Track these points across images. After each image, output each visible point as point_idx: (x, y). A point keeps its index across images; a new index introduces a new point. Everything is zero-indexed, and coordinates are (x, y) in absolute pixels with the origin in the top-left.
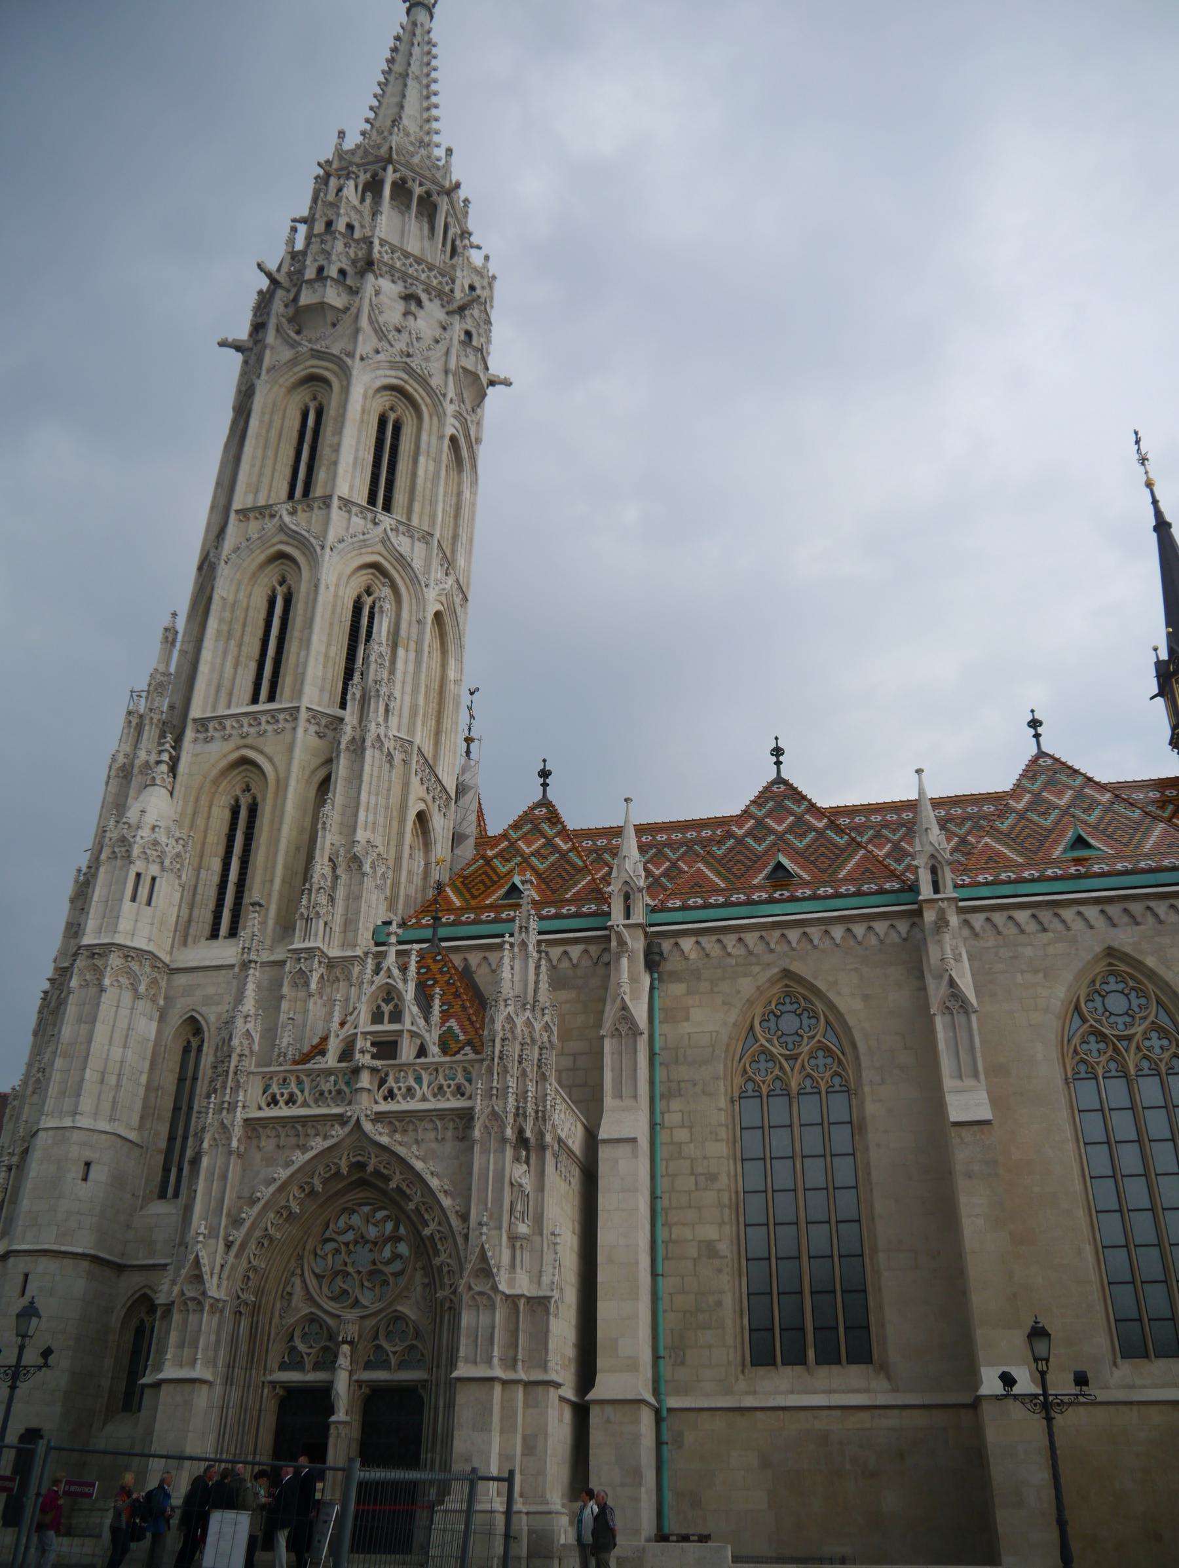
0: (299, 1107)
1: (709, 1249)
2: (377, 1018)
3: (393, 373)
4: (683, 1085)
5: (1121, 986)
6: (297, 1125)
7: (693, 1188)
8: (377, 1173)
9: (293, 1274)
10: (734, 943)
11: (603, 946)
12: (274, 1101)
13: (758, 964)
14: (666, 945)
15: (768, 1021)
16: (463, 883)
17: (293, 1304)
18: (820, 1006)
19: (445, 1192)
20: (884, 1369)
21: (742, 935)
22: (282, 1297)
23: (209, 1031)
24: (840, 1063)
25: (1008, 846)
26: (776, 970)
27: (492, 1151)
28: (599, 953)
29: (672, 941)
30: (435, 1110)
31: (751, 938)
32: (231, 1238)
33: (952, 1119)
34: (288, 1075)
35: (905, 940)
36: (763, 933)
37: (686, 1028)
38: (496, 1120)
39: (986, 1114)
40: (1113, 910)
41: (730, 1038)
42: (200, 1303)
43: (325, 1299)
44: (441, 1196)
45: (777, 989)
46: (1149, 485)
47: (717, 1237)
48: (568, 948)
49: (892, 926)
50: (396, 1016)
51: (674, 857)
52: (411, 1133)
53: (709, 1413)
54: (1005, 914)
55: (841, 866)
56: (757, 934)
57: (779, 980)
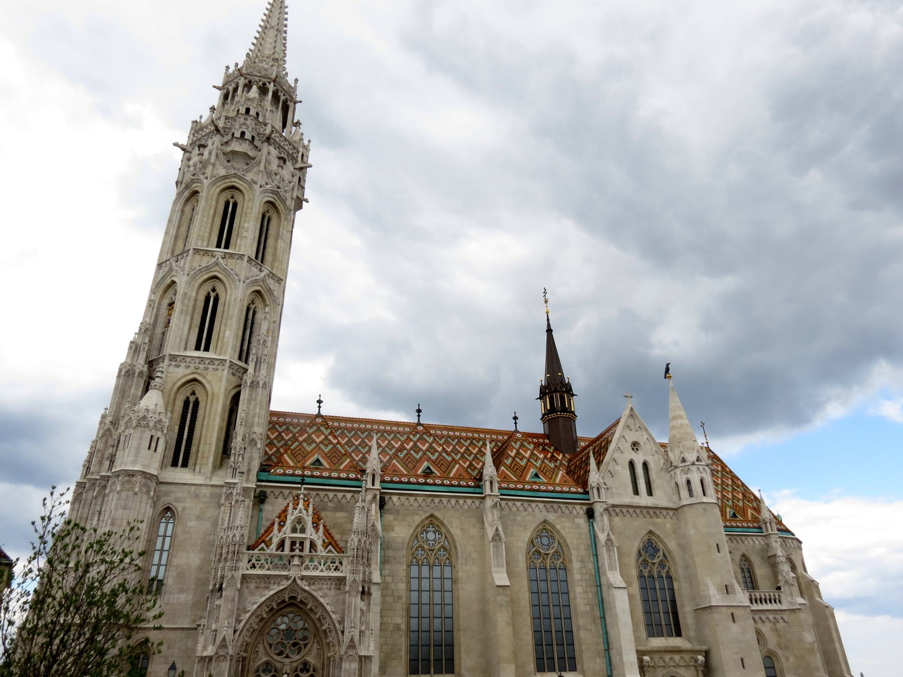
1: (397, 627)
2: (294, 530)
3: (271, 195)
5: (547, 534)
7: (392, 601)
8: (301, 602)
9: (259, 643)
12: (254, 566)
14: (387, 498)
18: (443, 530)
19: (333, 612)
21: (417, 498)
23: (178, 514)
24: (449, 554)
25: (511, 472)
26: (429, 514)
33: (497, 584)
34: (261, 555)
35: (477, 508)
36: (425, 498)
37: (392, 534)
39: (509, 584)
40: (548, 506)
41: (409, 540)
42: (225, 657)
44: (331, 614)
46: (547, 313)
49: (473, 502)
50: (303, 530)
52: (316, 585)
54: (513, 502)
55: (451, 471)
56: (422, 498)
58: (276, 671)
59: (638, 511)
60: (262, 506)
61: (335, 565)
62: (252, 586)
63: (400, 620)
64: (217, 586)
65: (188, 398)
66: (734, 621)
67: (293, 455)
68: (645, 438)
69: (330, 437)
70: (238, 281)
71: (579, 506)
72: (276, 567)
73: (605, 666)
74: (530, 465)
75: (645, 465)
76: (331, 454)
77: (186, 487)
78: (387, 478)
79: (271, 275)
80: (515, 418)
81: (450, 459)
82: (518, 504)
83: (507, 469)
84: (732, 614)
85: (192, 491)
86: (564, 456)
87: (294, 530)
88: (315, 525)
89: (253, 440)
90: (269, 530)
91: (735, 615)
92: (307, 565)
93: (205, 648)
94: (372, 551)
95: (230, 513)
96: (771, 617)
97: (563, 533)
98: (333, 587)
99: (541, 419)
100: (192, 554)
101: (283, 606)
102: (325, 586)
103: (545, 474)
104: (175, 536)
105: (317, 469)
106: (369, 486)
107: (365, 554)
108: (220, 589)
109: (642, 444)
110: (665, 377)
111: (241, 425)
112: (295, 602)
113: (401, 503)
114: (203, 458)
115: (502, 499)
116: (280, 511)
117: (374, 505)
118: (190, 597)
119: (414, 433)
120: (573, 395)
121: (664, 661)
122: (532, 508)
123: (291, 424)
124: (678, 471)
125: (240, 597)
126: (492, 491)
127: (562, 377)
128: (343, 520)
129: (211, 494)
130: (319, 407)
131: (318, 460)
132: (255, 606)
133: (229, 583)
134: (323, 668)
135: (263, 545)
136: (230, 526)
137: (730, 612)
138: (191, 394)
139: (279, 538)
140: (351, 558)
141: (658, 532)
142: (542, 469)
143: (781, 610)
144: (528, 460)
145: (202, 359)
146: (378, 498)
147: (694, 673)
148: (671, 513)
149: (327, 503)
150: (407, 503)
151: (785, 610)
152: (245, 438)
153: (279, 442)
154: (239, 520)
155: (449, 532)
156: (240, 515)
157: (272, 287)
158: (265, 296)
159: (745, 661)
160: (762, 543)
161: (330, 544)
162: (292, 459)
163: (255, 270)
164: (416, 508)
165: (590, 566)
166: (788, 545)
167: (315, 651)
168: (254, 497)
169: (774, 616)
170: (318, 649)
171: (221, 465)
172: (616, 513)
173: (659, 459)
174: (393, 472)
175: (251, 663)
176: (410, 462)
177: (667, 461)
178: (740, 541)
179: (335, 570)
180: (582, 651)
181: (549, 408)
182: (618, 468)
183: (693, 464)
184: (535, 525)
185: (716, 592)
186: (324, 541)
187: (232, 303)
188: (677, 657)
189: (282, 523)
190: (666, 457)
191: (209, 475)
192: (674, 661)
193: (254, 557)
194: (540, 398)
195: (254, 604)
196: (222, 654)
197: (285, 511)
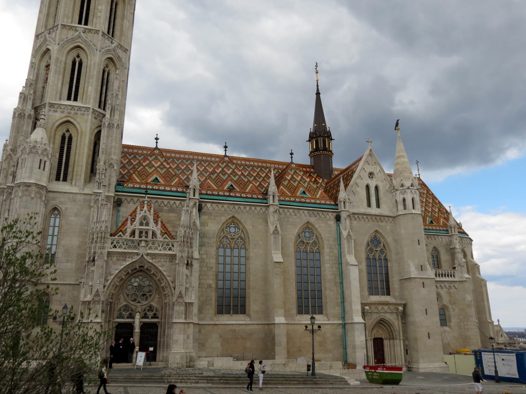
1: (210, 286)
2: (141, 224)
8: (147, 269)
9: (120, 293)
12: (115, 247)
14: (203, 205)
16: (138, 173)
18: (241, 227)
20: (249, 316)
24: (244, 242)
26: (231, 216)
33: (275, 261)
37: (207, 228)
39: (283, 261)
40: (311, 212)
42: (99, 302)
44: (167, 277)
48: (175, 201)
50: (147, 224)
51: (178, 163)
54: (287, 210)
55: (247, 188)
56: (227, 205)
58: (132, 311)
59: (369, 217)
60: (119, 208)
61: (169, 247)
62: (115, 259)
63: (211, 281)
64: (91, 258)
65: (64, 134)
66: (424, 287)
67: (139, 174)
68: (378, 170)
69: (164, 163)
70: (95, 50)
71: (332, 213)
72: (130, 247)
73: (340, 311)
74: (300, 186)
75: (377, 188)
76: (166, 175)
77: (66, 194)
78: (204, 192)
79: (119, 46)
80: (292, 154)
81: (246, 180)
82: (291, 211)
83: (284, 188)
84: (423, 283)
85: (71, 197)
86: (323, 180)
87: (141, 224)
88: (155, 221)
89: (111, 164)
90: (124, 223)
91: (425, 284)
92: (151, 247)
93: (85, 296)
94: (193, 239)
95: (98, 212)
96: (447, 285)
97: (319, 230)
98: (168, 260)
99: (309, 155)
100: (74, 238)
101: (135, 271)
102: (163, 260)
103: (310, 192)
104: (61, 226)
105: (156, 184)
106: (192, 196)
108: (94, 260)
109: (375, 174)
110: (395, 129)
111: (103, 153)
113: (213, 208)
114: (77, 175)
115: (280, 207)
116: (131, 212)
117: (194, 209)
119: (222, 162)
120: (332, 139)
121: (378, 310)
122: (300, 214)
123: (137, 154)
124: (398, 192)
125: (107, 265)
126: (274, 202)
127: (325, 126)
128: (174, 218)
129: (84, 200)
130: (157, 143)
131: (156, 179)
132: (117, 271)
134: (162, 310)
135: (121, 233)
136: (98, 221)
137: (422, 281)
138: (66, 132)
139: (131, 229)
140: (180, 243)
141: (381, 231)
142: (308, 188)
143: (454, 281)
144: (299, 183)
145: (73, 107)
146: (197, 204)
147: (396, 317)
148: (391, 219)
149: (163, 207)
150: (216, 208)
151: (457, 281)
152: (106, 163)
153: (129, 166)
154: (104, 217)
155: (244, 227)
156: (104, 214)
157: (120, 55)
158: (116, 62)
159: (428, 311)
160: (448, 240)
161: (166, 233)
163: (108, 42)
164: (222, 212)
165: (336, 251)
166: (464, 242)
167: (156, 299)
168: (114, 202)
169: (449, 285)
170: (159, 298)
171: (90, 181)
172: (355, 218)
173: (386, 184)
174: (208, 188)
175: (116, 306)
176: (219, 181)
177: (391, 185)
178: (433, 239)
179: (169, 250)
180: (327, 303)
181: (315, 147)
182: (358, 189)
183: (408, 188)
184: (301, 225)
185: (414, 269)
186: (161, 231)
187: (92, 67)
188: (386, 308)
189: (133, 220)
190: (391, 183)
191: (82, 187)
192: (384, 310)
194: (309, 141)
195: (116, 270)
196: (97, 300)
197: (135, 211)
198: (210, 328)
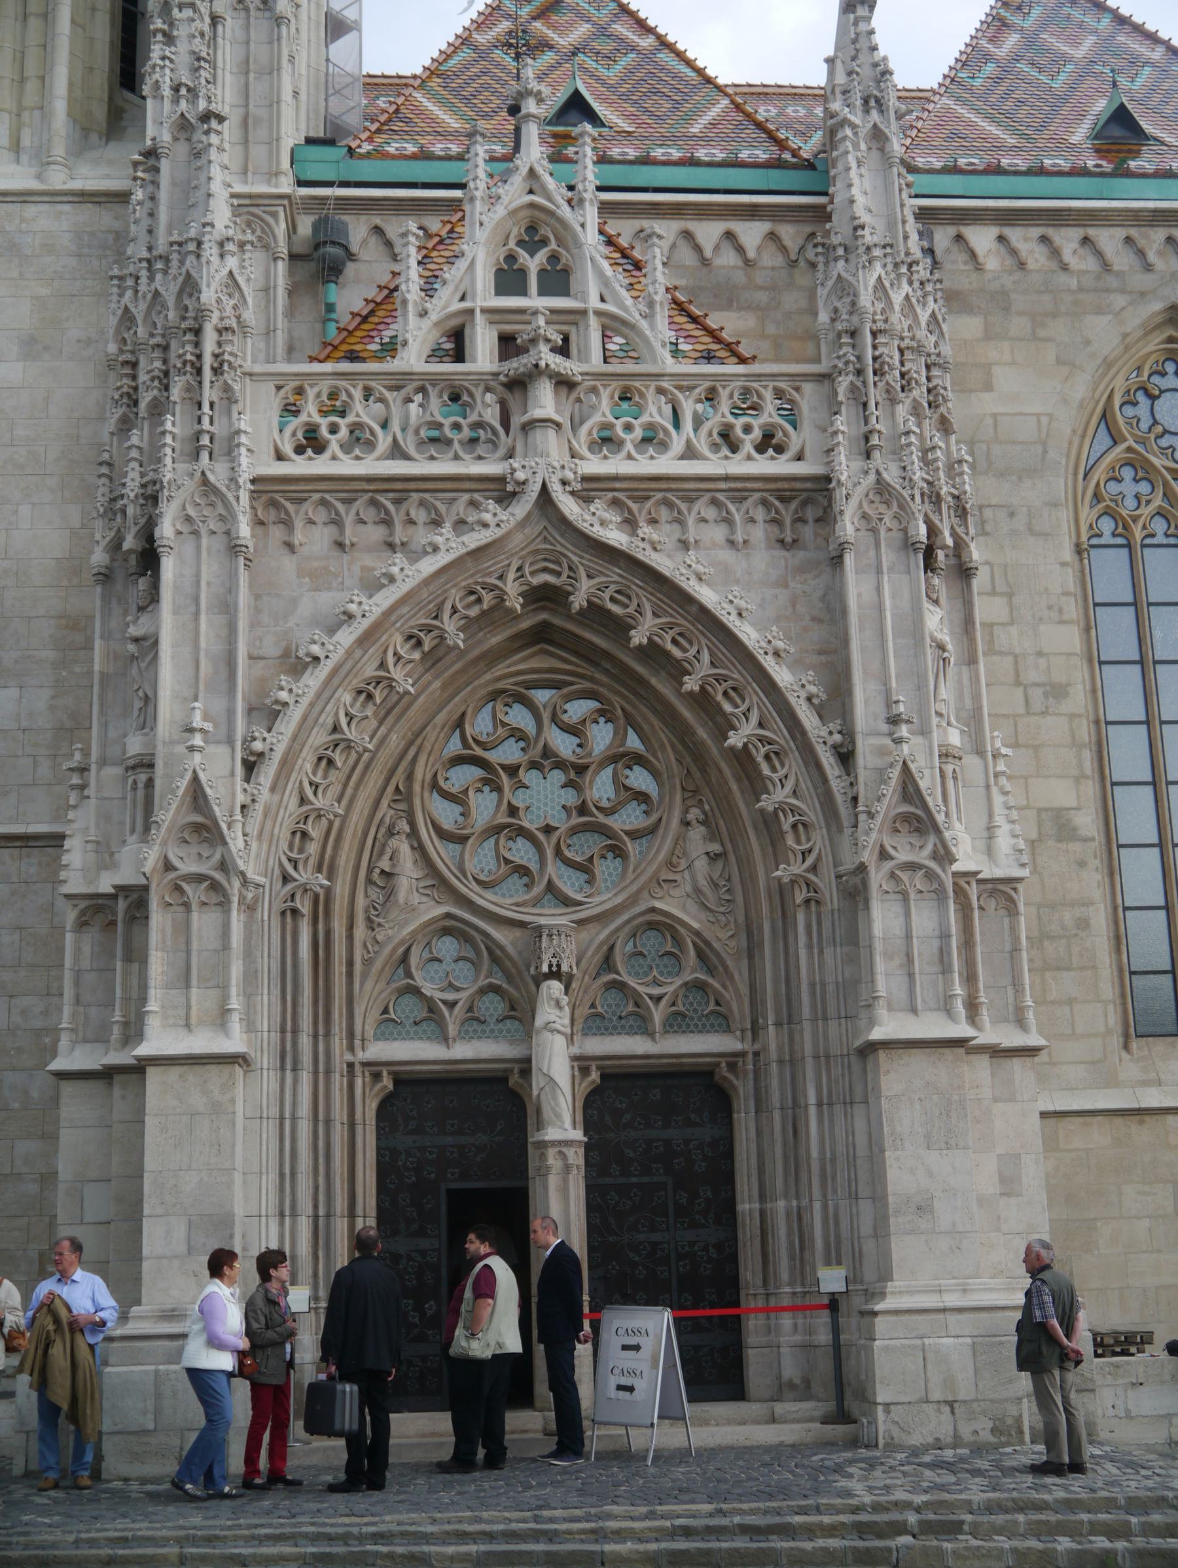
0: (378, 459)
4: (988, 513)
6: (381, 498)
7: (1022, 711)
8: (595, 613)
9: (391, 833)
10: (1075, 245)
11: (808, 229)
12: (312, 442)
13: (1123, 291)
15: (1135, 404)
17: (401, 896)
21: (1091, 232)
22: (370, 881)
27: (885, 570)
28: (800, 242)
29: (951, 231)
30: (727, 478)
31: (1109, 239)
32: (258, 746)
34: (344, 384)
36: (1133, 232)
38: (887, 503)
43: (474, 885)
44: (769, 663)
45: (1155, 343)
47: (1074, 804)
53: (1078, 1120)
56: (1121, 233)
57: (1158, 326)
64: (129, 543)
98: (759, 533)
100: (25, 510)
102: (718, 533)
107: (916, 368)
112: (557, 621)
118: (41, 699)
132: (346, 637)
133: (188, 519)
134: (752, 952)
136: (161, 247)
162: (452, 109)
170: (712, 858)
179: (761, 448)
193: (311, 393)
198: (1099, 1136)
